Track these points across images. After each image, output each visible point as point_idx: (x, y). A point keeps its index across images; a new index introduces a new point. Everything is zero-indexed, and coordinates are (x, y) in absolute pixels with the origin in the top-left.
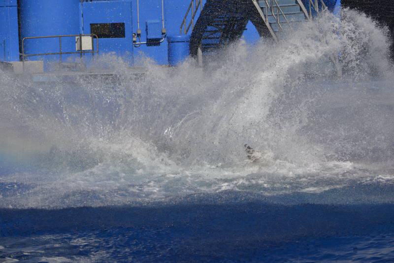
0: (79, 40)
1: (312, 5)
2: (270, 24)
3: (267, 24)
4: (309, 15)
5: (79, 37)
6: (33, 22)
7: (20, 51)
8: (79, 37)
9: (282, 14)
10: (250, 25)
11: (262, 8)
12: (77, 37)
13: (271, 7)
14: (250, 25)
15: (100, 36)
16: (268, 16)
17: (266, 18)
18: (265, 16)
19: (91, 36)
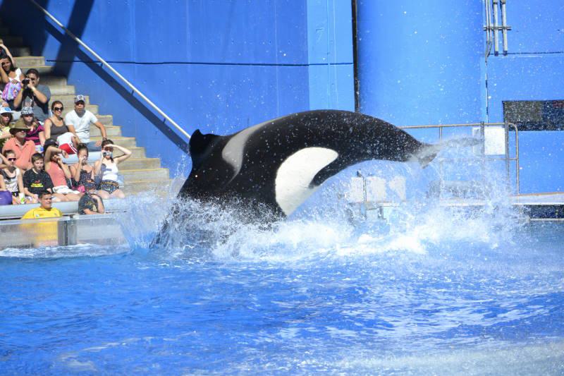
5: (479, 128)
8: (479, 128)
12: (475, 129)
15: (523, 127)
19: (504, 126)
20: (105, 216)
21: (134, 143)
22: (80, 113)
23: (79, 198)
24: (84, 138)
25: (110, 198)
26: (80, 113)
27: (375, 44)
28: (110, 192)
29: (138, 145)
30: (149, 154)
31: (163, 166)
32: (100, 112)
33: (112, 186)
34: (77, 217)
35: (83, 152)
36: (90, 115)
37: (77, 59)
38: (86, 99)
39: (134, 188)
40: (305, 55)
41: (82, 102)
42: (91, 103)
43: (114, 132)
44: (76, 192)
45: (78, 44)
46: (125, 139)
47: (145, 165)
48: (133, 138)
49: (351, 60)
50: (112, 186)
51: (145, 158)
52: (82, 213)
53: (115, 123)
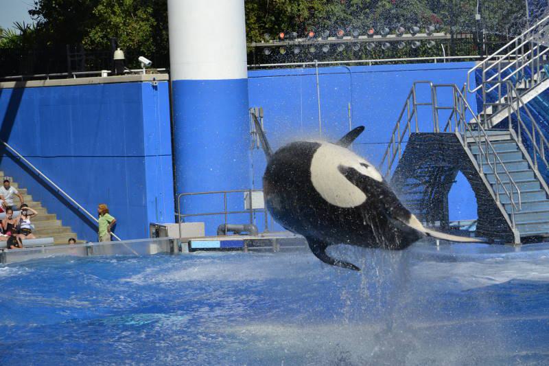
0: (248, 197)
1: (537, 152)
2: (485, 175)
3: (482, 175)
4: (534, 164)
6: (190, 174)
7: (176, 211)
9: (500, 163)
10: (460, 177)
11: (475, 156)
12: (245, 193)
13: (486, 154)
14: (460, 177)
16: (483, 165)
17: (480, 168)
18: (479, 165)
20: (24, 249)
21: (40, 205)
22: (7, 188)
23: (7, 239)
24: (10, 203)
25: (26, 239)
26: (7, 188)
27: (186, 144)
28: (26, 235)
29: (42, 206)
30: (49, 212)
31: (58, 219)
32: (19, 187)
33: (27, 232)
34: (6, 250)
35: (10, 211)
36: (13, 189)
37: (5, 155)
38: (10, 179)
39: (40, 233)
40: (143, 150)
41: (7, 181)
42: (14, 181)
43: (28, 199)
44: (6, 236)
45: (5, 146)
46: (35, 203)
47: (48, 218)
48: (39, 203)
49: (170, 153)
50: (27, 232)
51: (47, 214)
52: (9, 248)
53: (29, 193)
